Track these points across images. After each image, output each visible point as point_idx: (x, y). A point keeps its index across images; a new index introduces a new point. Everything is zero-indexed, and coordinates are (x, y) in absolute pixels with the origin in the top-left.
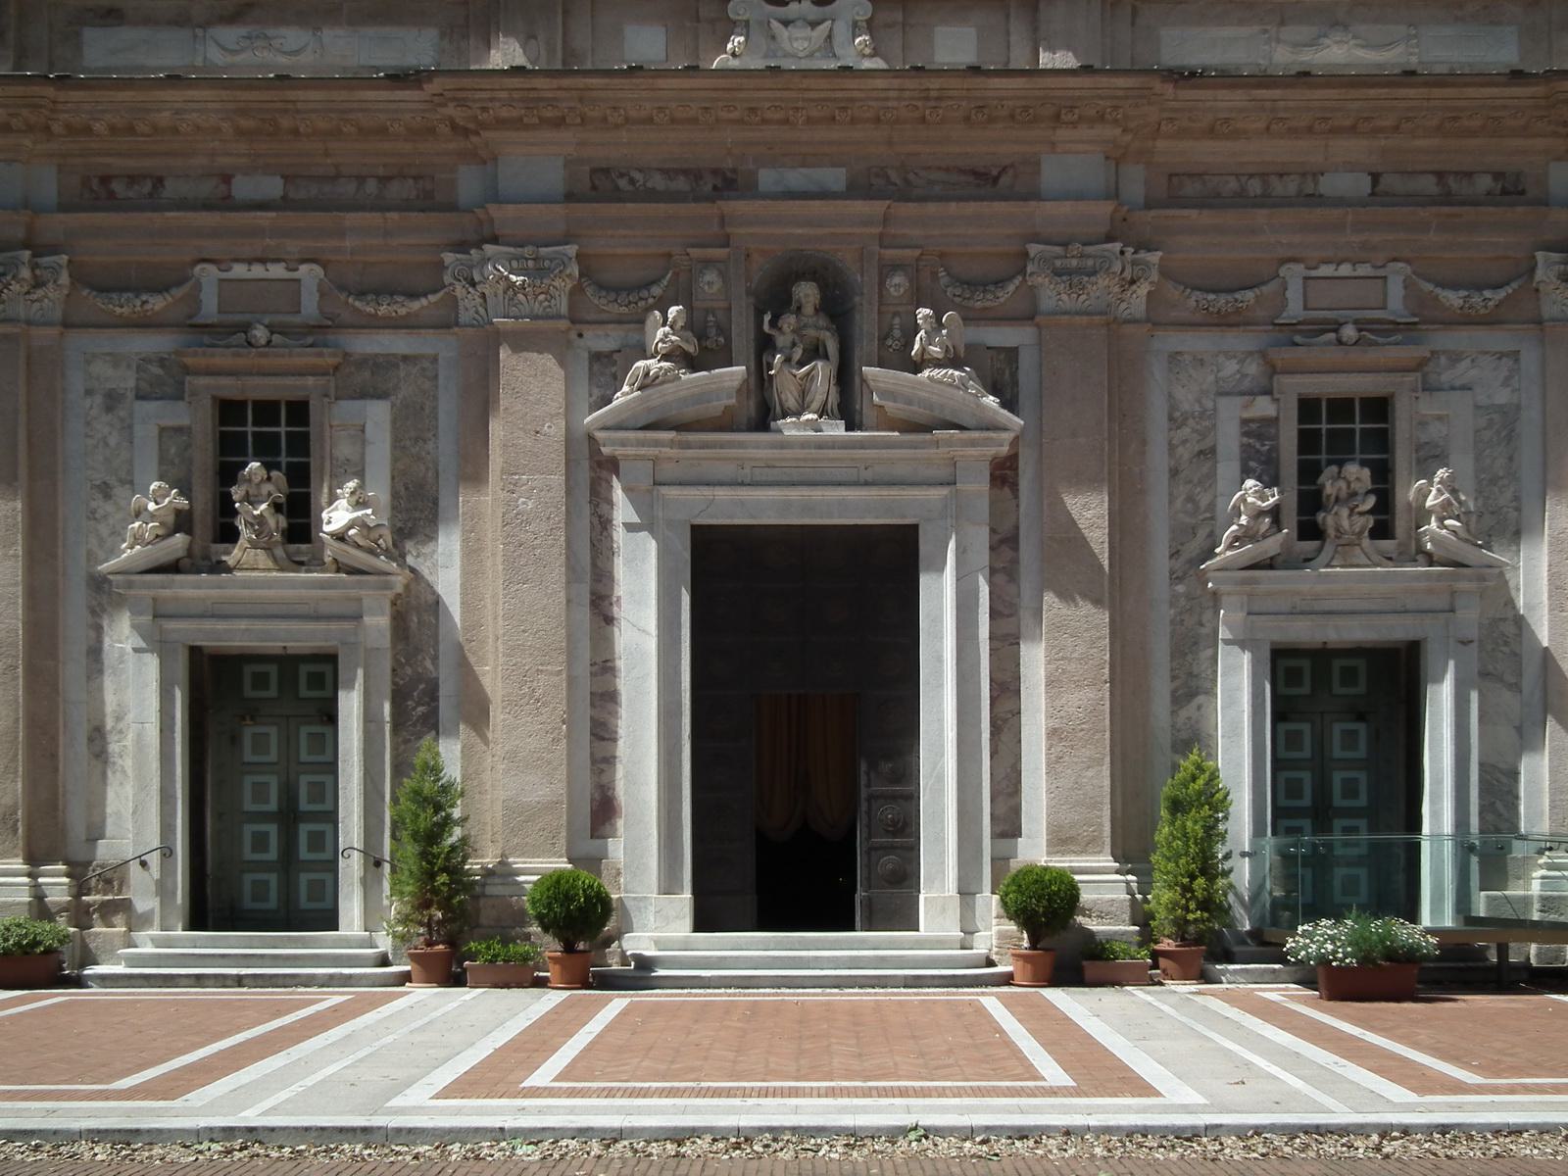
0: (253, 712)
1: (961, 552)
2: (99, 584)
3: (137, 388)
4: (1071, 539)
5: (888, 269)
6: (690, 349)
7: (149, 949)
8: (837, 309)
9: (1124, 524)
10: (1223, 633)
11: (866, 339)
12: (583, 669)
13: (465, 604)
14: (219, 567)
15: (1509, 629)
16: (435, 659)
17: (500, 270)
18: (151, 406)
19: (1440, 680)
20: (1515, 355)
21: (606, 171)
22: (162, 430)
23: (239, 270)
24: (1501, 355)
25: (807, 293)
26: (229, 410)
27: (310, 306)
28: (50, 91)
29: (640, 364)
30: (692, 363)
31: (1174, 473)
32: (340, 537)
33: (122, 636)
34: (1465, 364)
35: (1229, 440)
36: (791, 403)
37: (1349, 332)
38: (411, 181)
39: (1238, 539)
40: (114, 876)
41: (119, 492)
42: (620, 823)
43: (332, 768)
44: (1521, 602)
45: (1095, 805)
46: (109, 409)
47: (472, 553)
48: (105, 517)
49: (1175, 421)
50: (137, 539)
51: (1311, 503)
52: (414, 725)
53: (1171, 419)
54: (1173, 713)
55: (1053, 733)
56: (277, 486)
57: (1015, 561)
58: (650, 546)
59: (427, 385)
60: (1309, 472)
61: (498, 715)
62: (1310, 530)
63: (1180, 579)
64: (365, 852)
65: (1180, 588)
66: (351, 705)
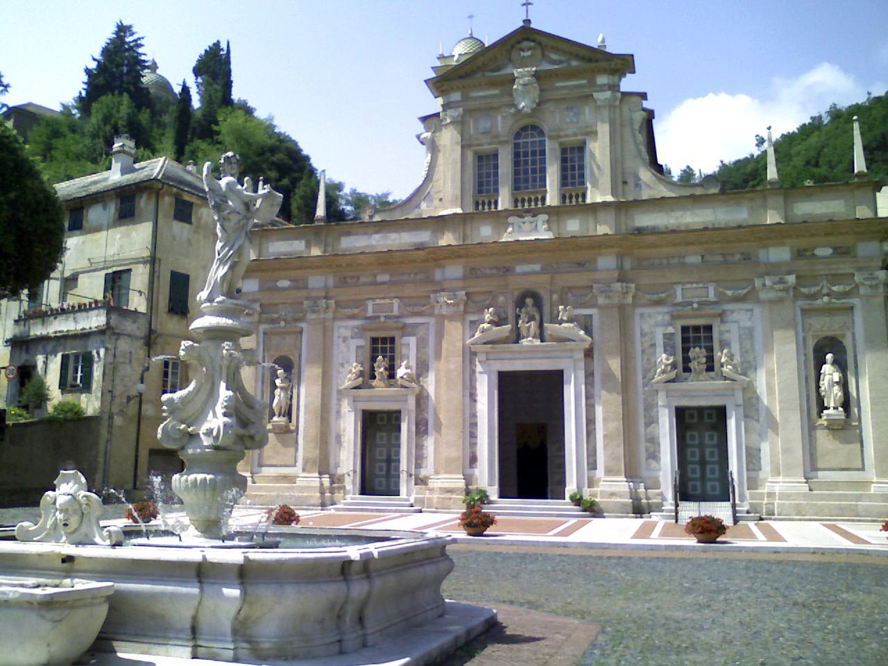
0: (380, 429)
1: (575, 378)
2: (339, 392)
4: (608, 375)
5: (552, 292)
6: (496, 320)
7: (349, 501)
8: (538, 304)
9: (625, 368)
10: (660, 403)
11: (546, 317)
12: (467, 415)
13: (436, 397)
14: (371, 387)
15: (754, 401)
16: (427, 413)
17: (444, 298)
18: (354, 340)
19: (730, 418)
20: (752, 310)
21: (474, 269)
22: (357, 347)
23: (378, 301)
24: (747, 310)
25: (529, 301)
26: (374, 341)
27: (396, 312)
28: (332, 258)
29: (482, 326)
30: (497, 324)
31: (643, 351)
32: (402, 378)
33: (346, 407)
34: (735, 314)
35: (660, 341)
36: (525, 334)
37: (695, 305)
39: (663, 372)
40: (341, 479)
41: (346, 365)
42: (478, 464)
43: (399, 446)
44: (758, 391)
45: (618, 459)
47: (437, 381)
49: (643, 335)
50: (350, 379)
51: (686, 360)
53: (641, 334)
54: (645, 430)
55: (605, 436)
56: (386, 363)
57: (593, 381)
58: (485, 377)
60: (686, 350)
61: (444, 430)
62: (687, 369)
63: (646, 386)
64: (407, 472)
65: (646, 389)
66: (404, 427)
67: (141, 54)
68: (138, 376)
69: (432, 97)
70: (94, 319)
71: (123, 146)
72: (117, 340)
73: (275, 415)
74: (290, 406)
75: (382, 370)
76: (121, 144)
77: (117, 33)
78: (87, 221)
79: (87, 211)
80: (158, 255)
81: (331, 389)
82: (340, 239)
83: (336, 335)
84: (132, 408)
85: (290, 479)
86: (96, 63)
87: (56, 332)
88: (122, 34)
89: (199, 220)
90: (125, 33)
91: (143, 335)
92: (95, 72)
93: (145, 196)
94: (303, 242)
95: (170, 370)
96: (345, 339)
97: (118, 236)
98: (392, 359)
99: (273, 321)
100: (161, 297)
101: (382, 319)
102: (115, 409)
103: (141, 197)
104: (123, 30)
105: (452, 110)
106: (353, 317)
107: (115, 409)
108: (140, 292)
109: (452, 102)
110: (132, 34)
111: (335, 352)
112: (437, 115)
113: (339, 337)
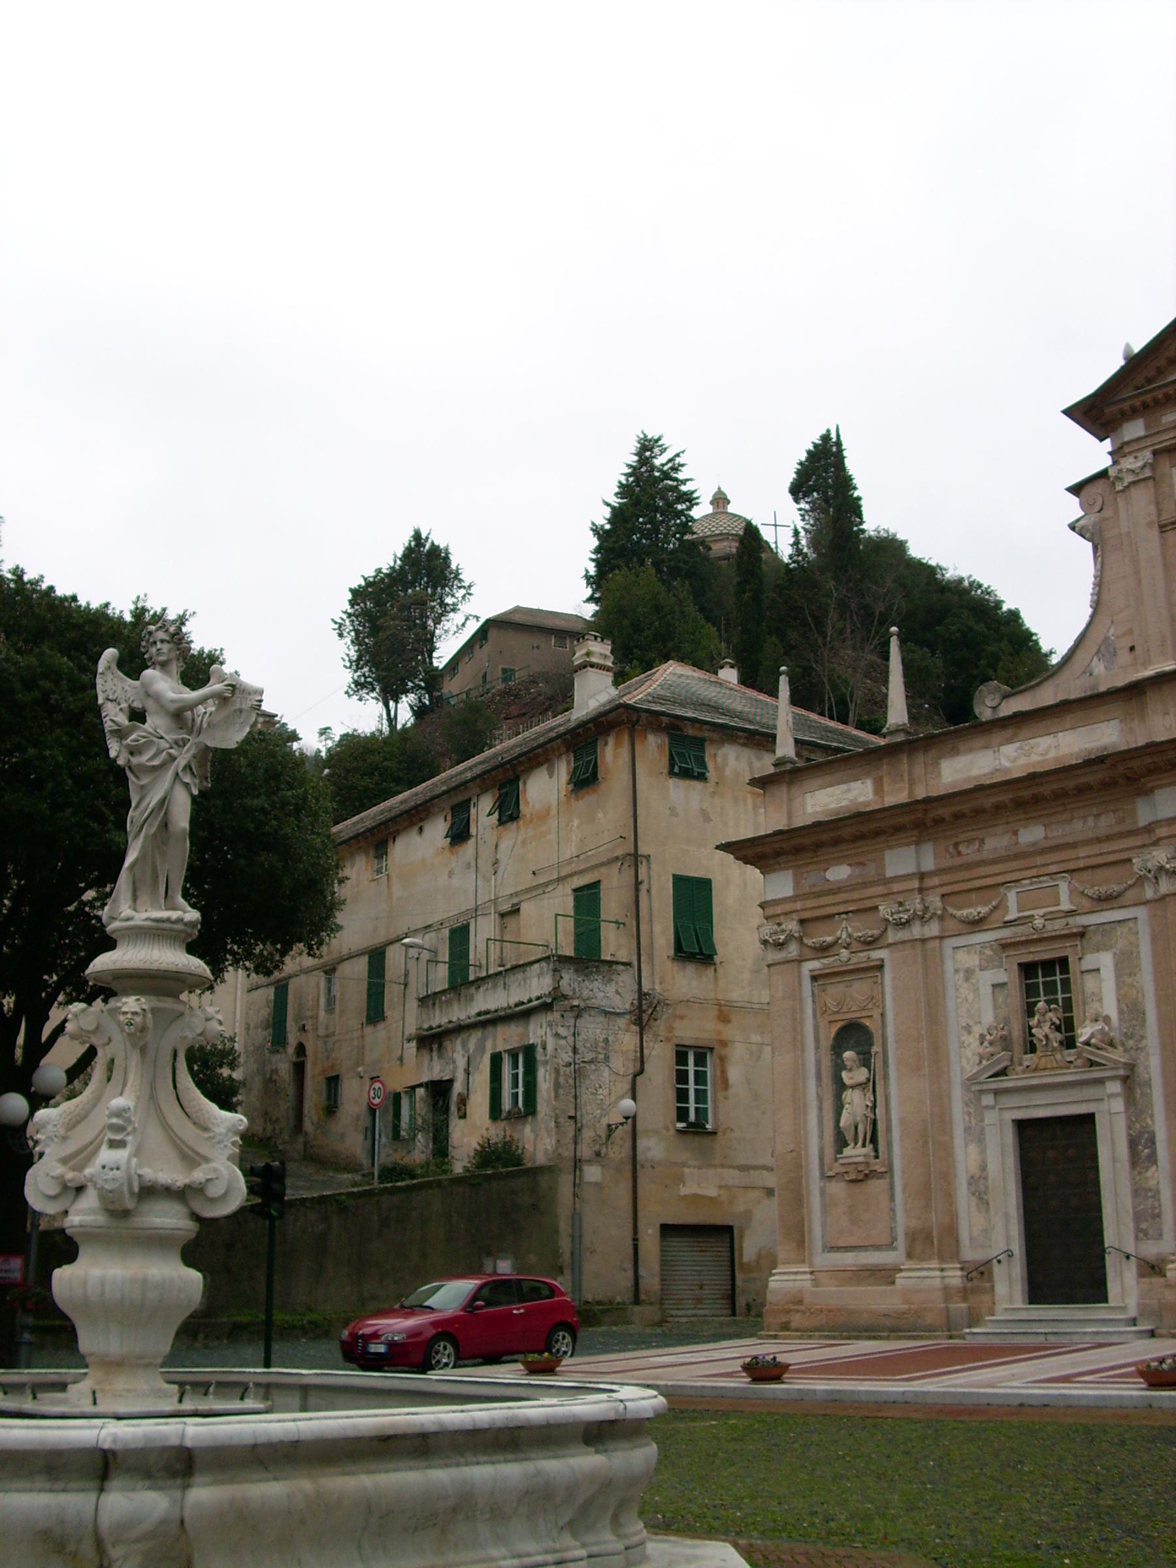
3: (980, 964)
16: (1152, 1116)
22: (994, 986)
26: (1028, 970)
32: (1087, 1043)
38: (1112, 814)
46: (967, 979)
48: (969, 1045)
52: (1143, 1162)
59: (1133, 938)
67: (684, 482)
68: (626, 1085)
69: (1097, 441)
70: (535, 981)
71: (588, 654)
72: (577, 1017)
73: (846, 1145)
74: (874, 1122)
75: (1046, 1028)
76: (584, 651)
77: (640, 453)
78: (527, 803)
79: (525, 783)
80: (643, 849)
81: (949, 1082)
82: (939, 764)
83: (949, 966)
84: (618, 1151)
85: (886, 1274)
86: (609, 509)
87: (479, 1014)
88: (648, 454)
89: (720, 770)
90: (651, 450)
91: (628, 1006)
92: (608, 527)
93: (611, 741)
94: (869, 783)
95: (691, 1068)
96: (969, 973)
97: (576, 823)
98: (1068, 1005)
99: (824, 950)
100: (657, 928)
101: (1038, 922)
102: (585, 1151)
103: (606, 744)
104: (647, 447)
105: (1131, 459)
106: (976, 924)
107: (585, 1151)
108: (617, 922)
109: (1128, 443)
110: (663, 451)
111: (951, 1003)
112: (1103, 474)
113: (957, 971)
